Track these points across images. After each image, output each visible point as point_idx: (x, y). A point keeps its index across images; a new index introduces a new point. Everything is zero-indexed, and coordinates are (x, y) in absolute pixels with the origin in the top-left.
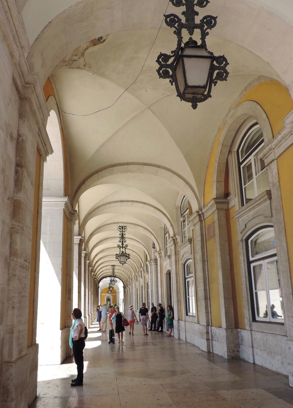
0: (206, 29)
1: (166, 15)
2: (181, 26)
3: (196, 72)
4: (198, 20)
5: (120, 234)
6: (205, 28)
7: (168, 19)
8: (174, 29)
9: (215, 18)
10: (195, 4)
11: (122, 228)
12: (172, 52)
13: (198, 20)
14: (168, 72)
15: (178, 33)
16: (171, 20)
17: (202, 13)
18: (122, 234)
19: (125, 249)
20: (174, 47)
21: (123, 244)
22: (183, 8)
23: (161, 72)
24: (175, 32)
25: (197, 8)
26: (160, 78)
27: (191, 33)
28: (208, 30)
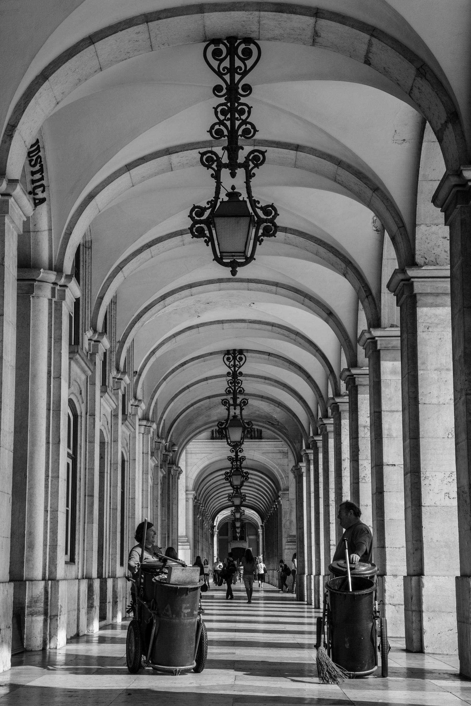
2: (221, 166)
4: (241, 159)
6: (250, 168)
7: (205, 157)
10: (240, 135)
15: (217, 176)
16: (208, 160)
22: (225, 141)
23: (194, 228)
27: (233, 175)
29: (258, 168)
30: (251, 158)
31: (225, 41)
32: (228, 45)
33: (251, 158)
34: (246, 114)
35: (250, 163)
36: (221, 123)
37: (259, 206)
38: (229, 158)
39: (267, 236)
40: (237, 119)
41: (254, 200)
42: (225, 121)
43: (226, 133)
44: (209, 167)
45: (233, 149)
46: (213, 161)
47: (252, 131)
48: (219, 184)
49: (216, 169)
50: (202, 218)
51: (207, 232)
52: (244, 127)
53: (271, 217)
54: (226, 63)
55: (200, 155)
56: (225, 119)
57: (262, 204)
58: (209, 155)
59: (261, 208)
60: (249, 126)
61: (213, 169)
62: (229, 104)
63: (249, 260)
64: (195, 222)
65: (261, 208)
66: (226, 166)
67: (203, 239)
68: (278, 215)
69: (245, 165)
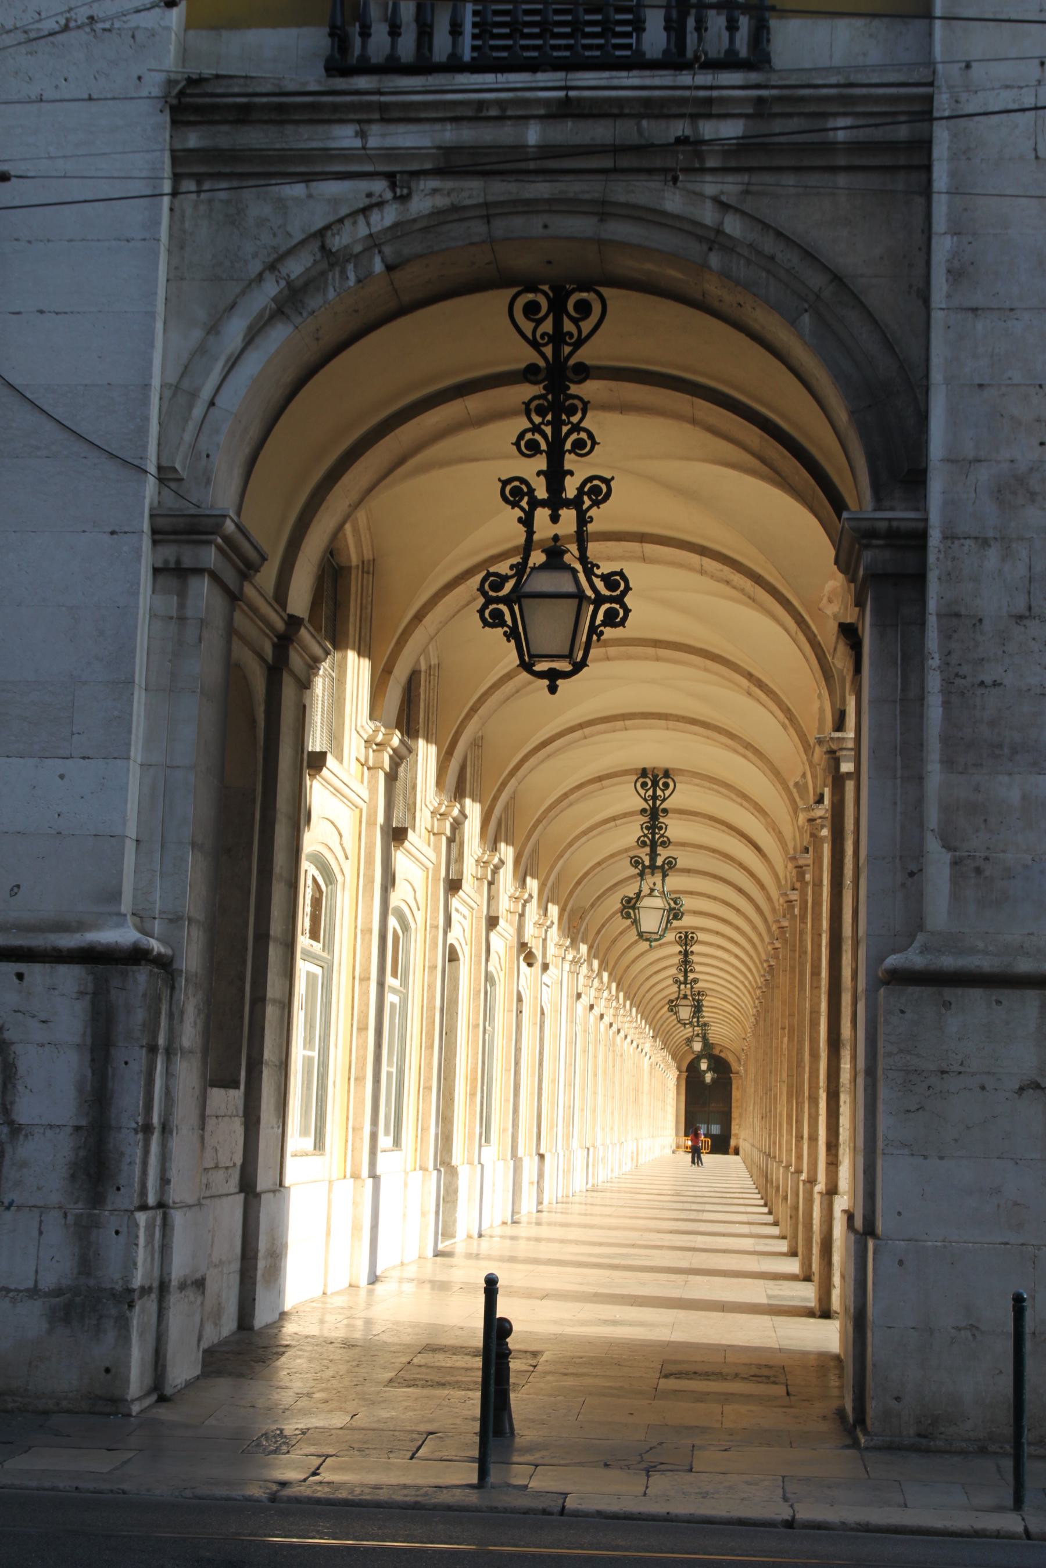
0: (589, 508)
1: (503, 478)
2: (535, 503)
4: (571, 492)
6: (585, 507)
7: (508, 488)
8: (518, 513)
14: (501, 614)
15: (527, 522)
16: (515, 492)
22: (541, 463)
23: (487, 612)
24: (520, 520)
25: (570, 461)
27: (555, 518)
30: (586, 489)
31: (546, 288)
32: (551, 295)
33: (586, 489)
34: (579, 415)
35: (586, 498)
36: (536, 429)
38: (549, 489)
40: (564, 423)
41: (591, 563)
42: (543, 427)
43: (544, 446)
44: (515, 504)
45: (555, 475)
47: (589, 443)
48: (530, 533)
49: (526, 507)
52: (574, 436)
53: (618, 592)
54: (547, 326)
55: (500, 485)
56: (542, 423)
58: (517, 483)
60: (583, 435)
62: (550, 397)
64: (489, 601)
66: (543, 503)
67: (500, 631)
69: (576, 503)
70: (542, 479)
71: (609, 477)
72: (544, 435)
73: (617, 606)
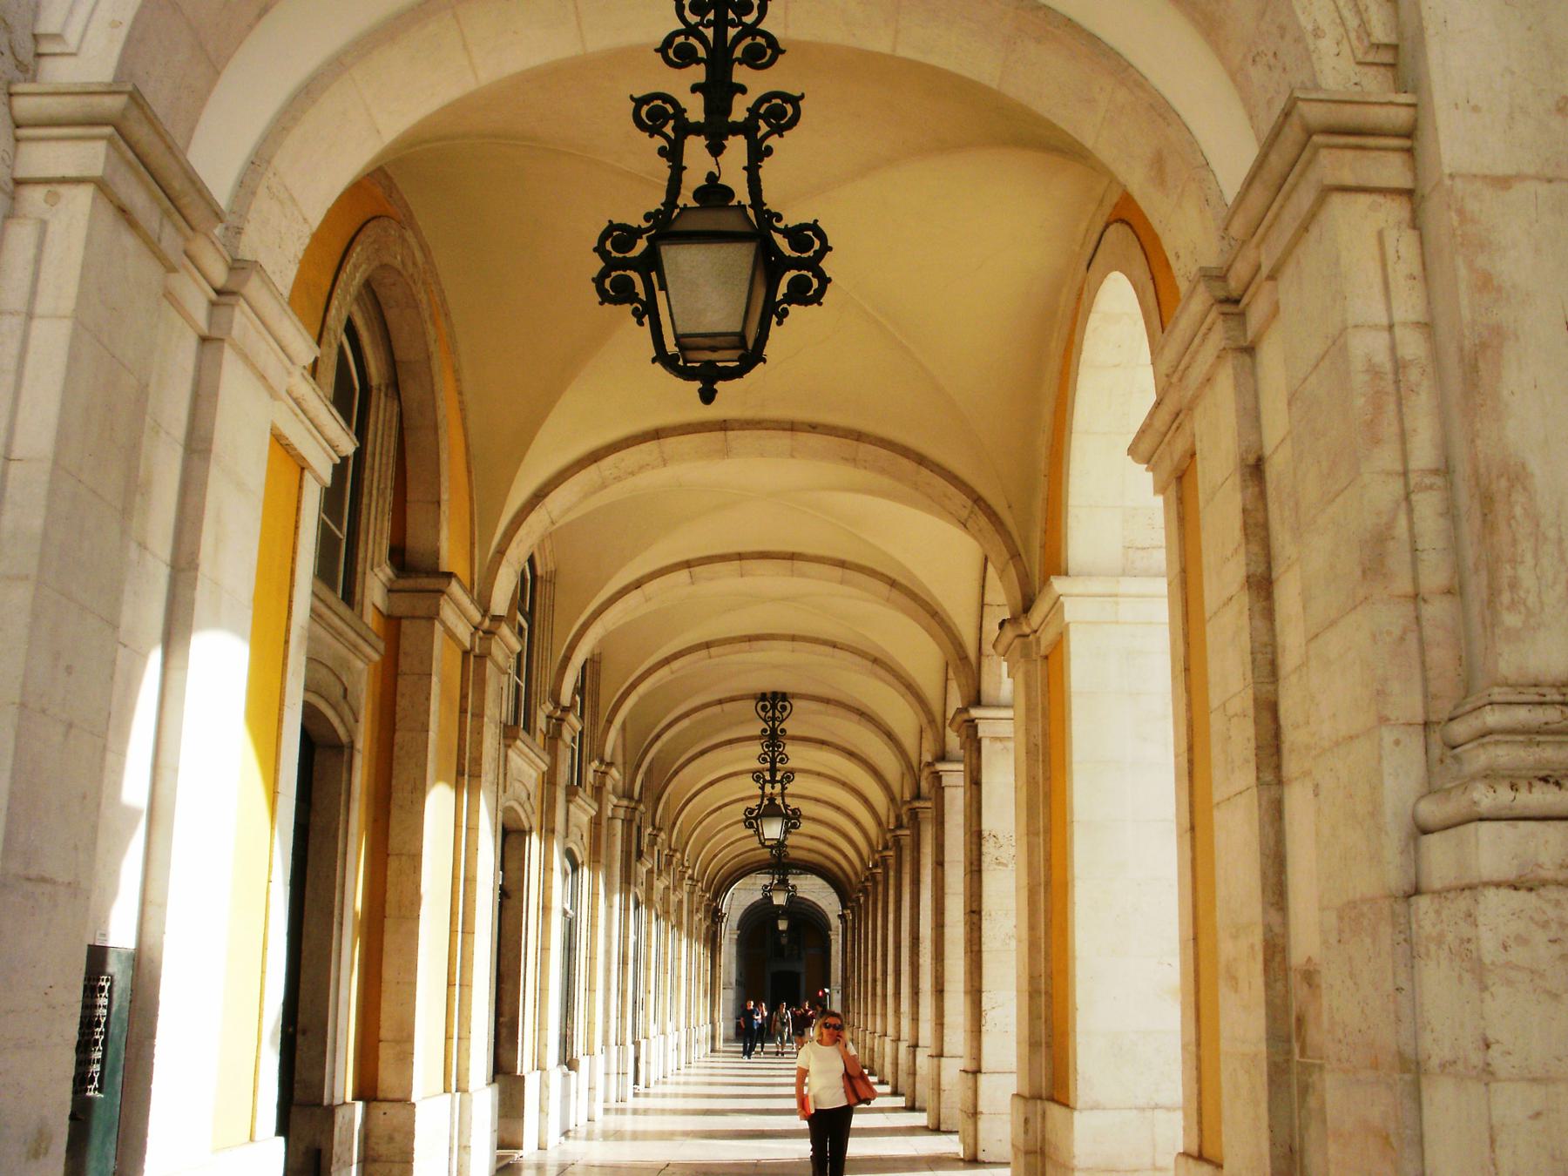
2: (685, 128)
3: (706, 287)
4: (739, 113)
5: (764, 730)
6: (759, 135)
7: (645, 109)
9: (795, 101)
10: (737, 59)
11: (774, 707)
12: (648, 217)
13: (739, 111)
14: (631, 281)
15: (673, 154)
16: (654, 114)
17: (754, 83)
18: (774, 730)
19: (784, 788)
20: (656, 201)
21: (773, 770)
22: (698, 73)
23: (607, 282)
24: (662, 152)
25: (740, 74)
26: (601, 303)
27: (716, 149)
28: (773, 141)
29: (781, 136)
35: (761, 122)
37: (781, 225)
39: (800, 303)
41: (768, 211)
43: (702, 53)
44: (654, 131)
45: (718, 91)
46: (666, 117)
48: (677, 170)
49: (672, 135)
50: (630, 255)
51: (640, 288)
52: (748, 41)
57: (791, 219)
58: (659, 102)
59: (786, 232)
60: (760, 40)
61: (666, 137)
63: (751, 356)
65: (786, 232)
66: (697, 129)
67: (627, 308)
68: (830, 249)
70: (699, 99)
71: (797, 94)
72: (702, 39)
73: (810, 274)
